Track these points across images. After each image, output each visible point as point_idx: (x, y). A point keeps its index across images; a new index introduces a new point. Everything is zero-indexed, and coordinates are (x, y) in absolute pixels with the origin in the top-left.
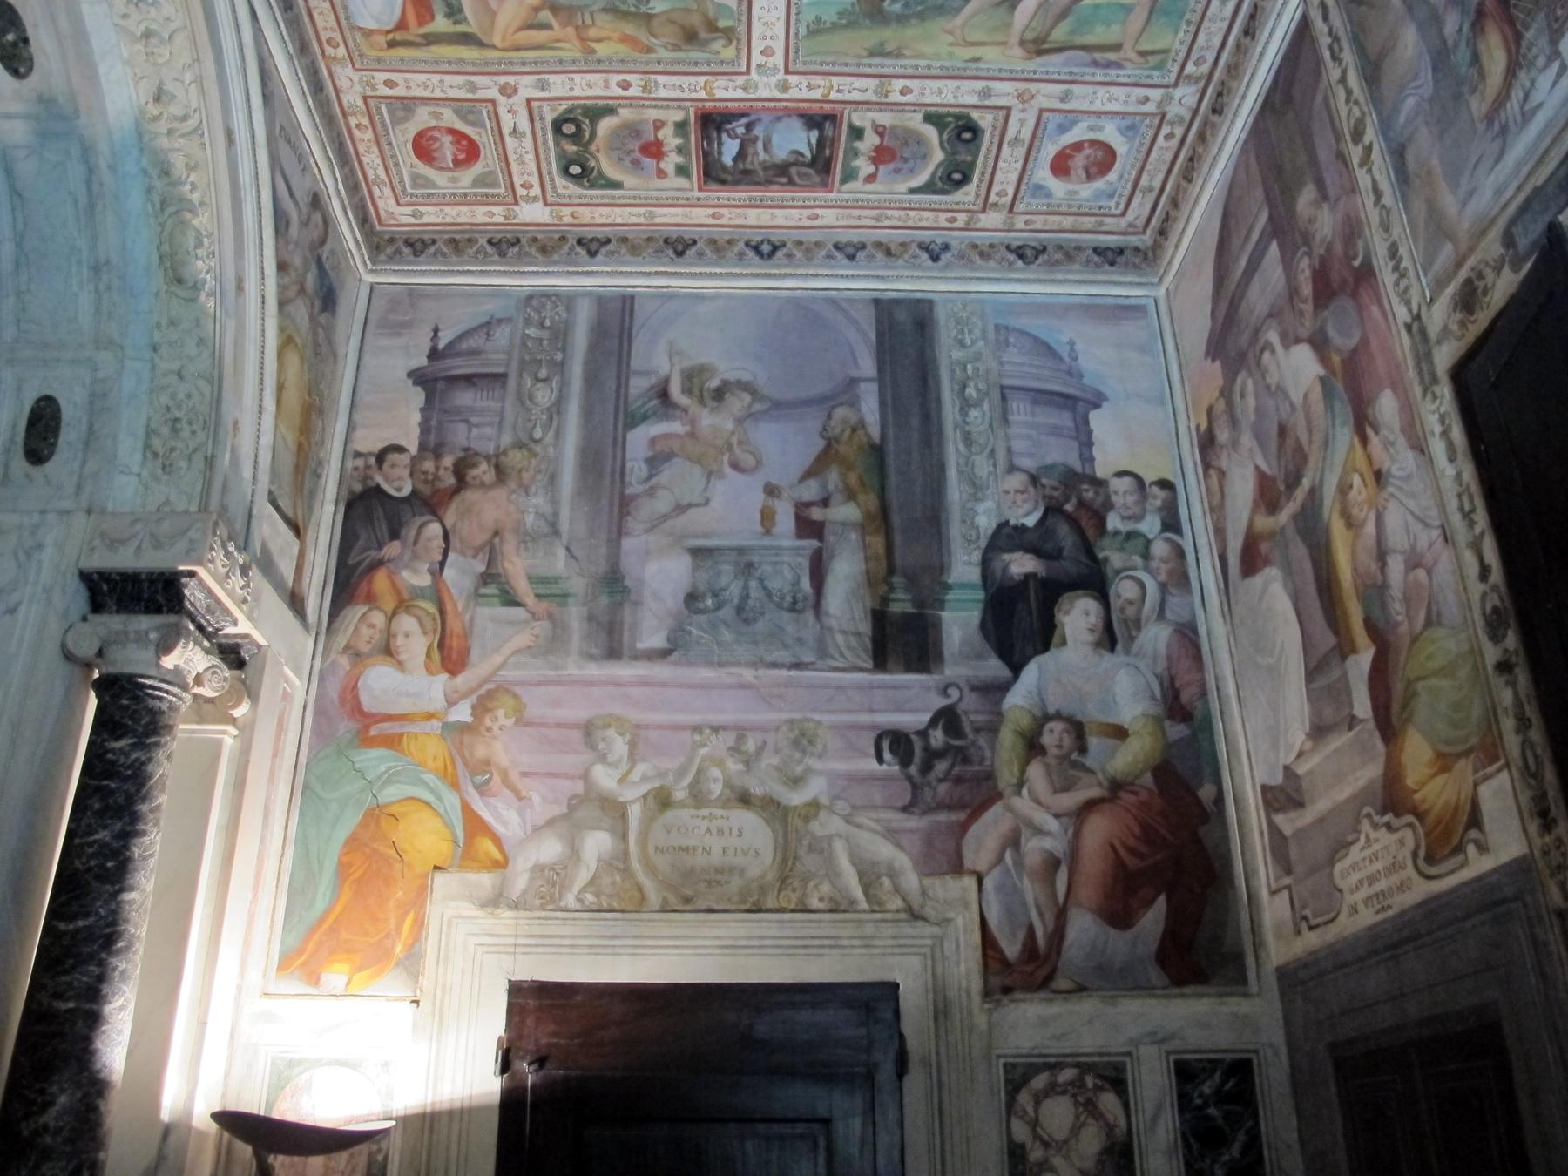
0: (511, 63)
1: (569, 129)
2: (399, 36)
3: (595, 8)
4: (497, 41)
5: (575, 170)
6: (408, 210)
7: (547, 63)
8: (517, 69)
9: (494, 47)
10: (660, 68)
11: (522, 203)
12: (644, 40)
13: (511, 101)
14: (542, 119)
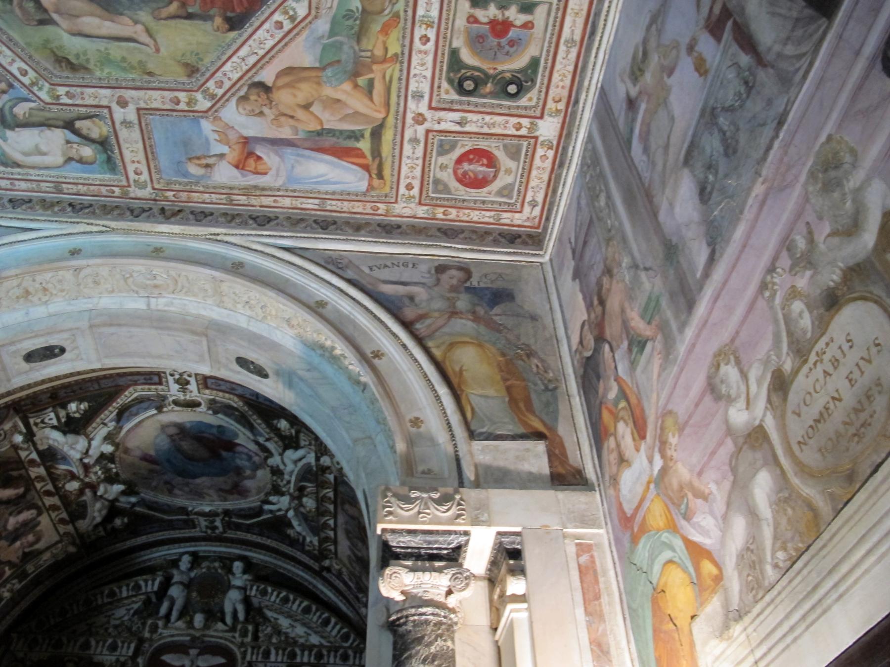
0: (397, 112)
1: (469, 85)
2: (374, 172)
3: (357, 48)
4: (381, 116)
5: (512, 89)
6: (527, 209)
7: (399, 88)
8: (401, 109)
9: (384, 119)
10: (410, 13)
11: (537, 134)
12: (387, 18)
13: (429, 120)
14: (452, 102)
